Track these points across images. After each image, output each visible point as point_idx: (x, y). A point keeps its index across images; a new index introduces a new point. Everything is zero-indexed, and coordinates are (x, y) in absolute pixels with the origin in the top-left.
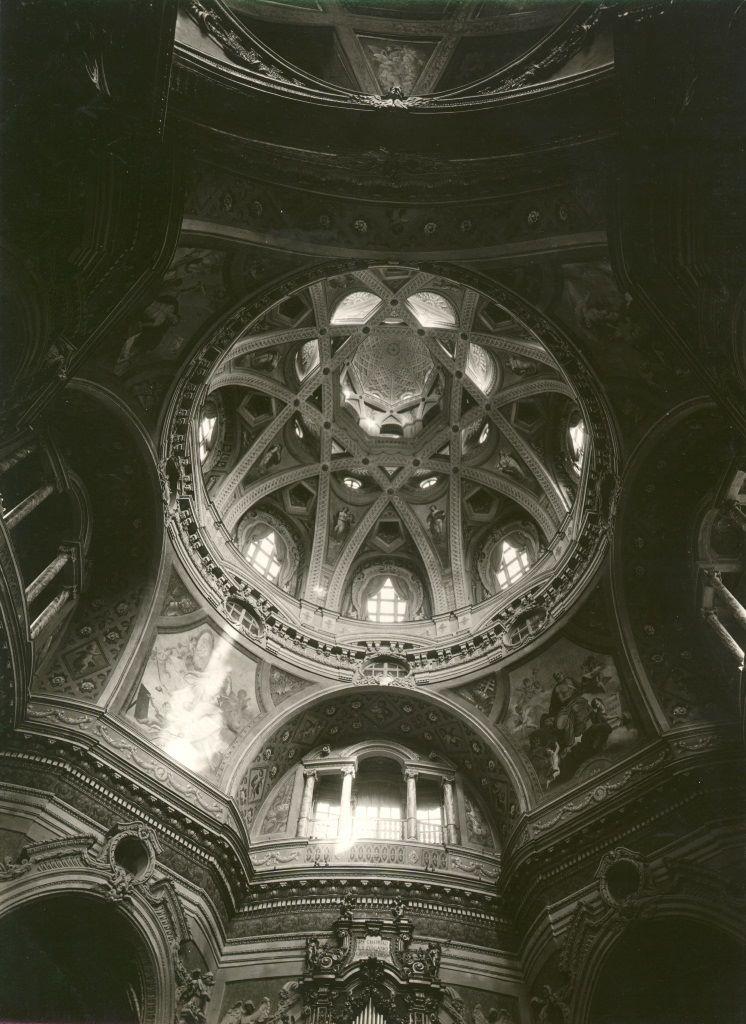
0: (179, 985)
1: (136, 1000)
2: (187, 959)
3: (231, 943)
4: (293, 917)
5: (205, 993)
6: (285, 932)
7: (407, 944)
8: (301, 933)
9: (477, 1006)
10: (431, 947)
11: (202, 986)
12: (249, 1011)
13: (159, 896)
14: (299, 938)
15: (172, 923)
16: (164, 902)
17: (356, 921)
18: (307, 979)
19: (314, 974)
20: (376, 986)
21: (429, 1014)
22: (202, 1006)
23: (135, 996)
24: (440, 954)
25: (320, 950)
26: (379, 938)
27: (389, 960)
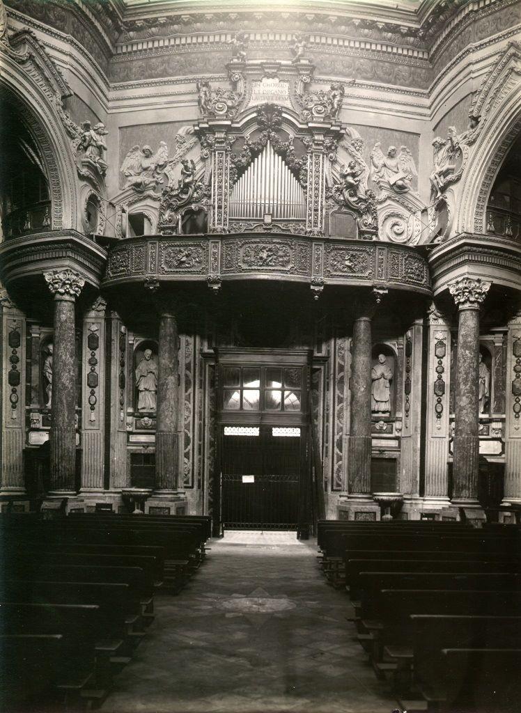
0: (73, 138)
1: (34, 155)
2: (72, 112)
3: (115, 88)
4: (178, 57)
5: (100, 143)
6: (171, 75)
7: (306, 86)
8: (190, 76)
9: (376, 145)
10: (333, 89)
11: (96, 137)
12: (148, 154)
13: (24, 52)
14: (189, 81)
15: (47, 79)
16: (31, 57)
17: (251, 62)
18: (201, 125)
19: (209, 121)
20: (273, 130)
21: (327, 155)
22: (100, 154)
23: (31, 151)
24: (342, 95)
25: (214, 95)
26: (277, 80)
27: (288, 104)
